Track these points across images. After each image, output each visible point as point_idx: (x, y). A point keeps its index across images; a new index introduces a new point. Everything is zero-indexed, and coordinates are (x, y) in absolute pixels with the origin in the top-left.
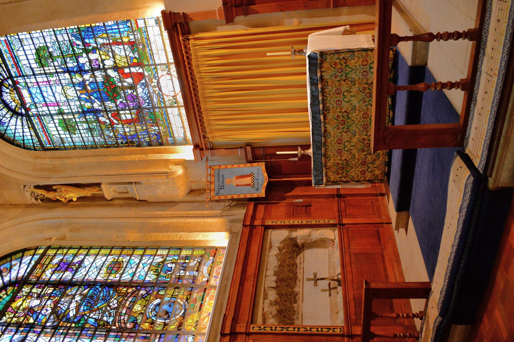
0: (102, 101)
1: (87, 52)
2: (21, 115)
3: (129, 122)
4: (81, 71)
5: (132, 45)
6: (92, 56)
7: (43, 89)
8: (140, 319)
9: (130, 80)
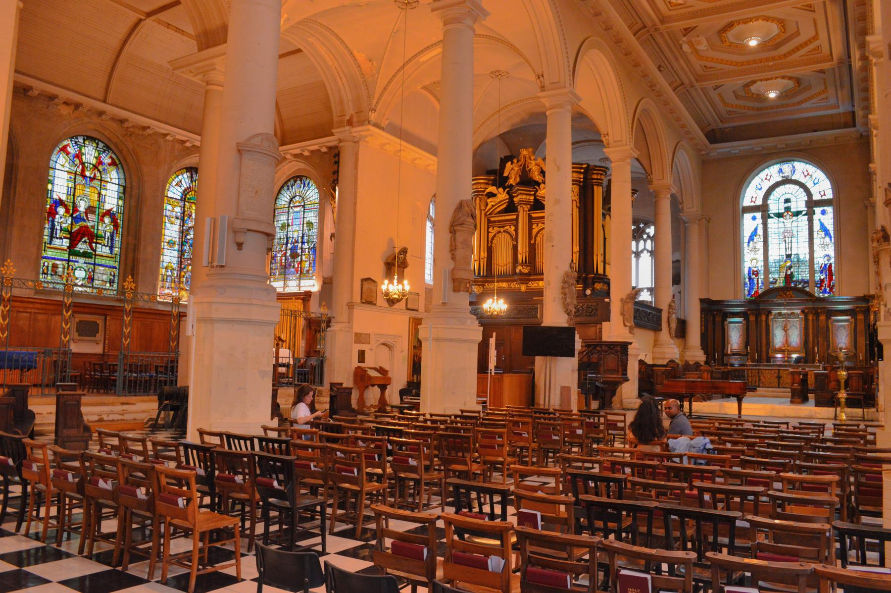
0: (291, 249)
1: (309, 248)
2: (290, 203)
3: (281, 260)
4: (303, 243)
5: (308, 271)
6: (307, 250)
7: (299, 220)
8: (185, 270)
9: (296, 266)
